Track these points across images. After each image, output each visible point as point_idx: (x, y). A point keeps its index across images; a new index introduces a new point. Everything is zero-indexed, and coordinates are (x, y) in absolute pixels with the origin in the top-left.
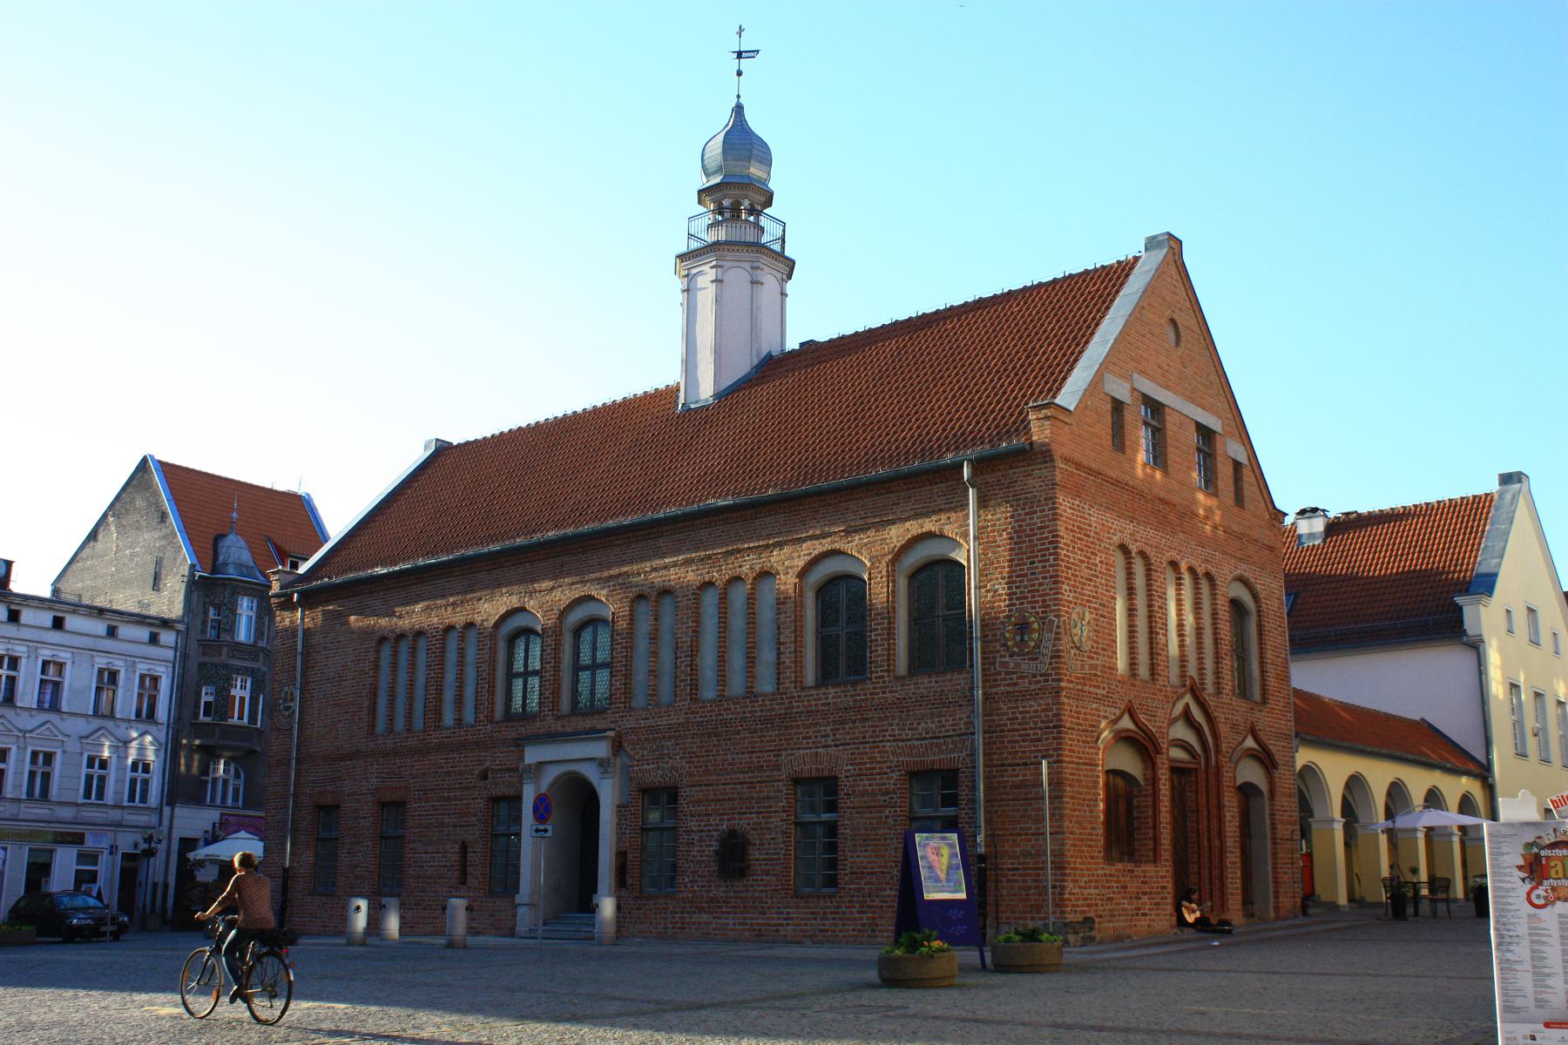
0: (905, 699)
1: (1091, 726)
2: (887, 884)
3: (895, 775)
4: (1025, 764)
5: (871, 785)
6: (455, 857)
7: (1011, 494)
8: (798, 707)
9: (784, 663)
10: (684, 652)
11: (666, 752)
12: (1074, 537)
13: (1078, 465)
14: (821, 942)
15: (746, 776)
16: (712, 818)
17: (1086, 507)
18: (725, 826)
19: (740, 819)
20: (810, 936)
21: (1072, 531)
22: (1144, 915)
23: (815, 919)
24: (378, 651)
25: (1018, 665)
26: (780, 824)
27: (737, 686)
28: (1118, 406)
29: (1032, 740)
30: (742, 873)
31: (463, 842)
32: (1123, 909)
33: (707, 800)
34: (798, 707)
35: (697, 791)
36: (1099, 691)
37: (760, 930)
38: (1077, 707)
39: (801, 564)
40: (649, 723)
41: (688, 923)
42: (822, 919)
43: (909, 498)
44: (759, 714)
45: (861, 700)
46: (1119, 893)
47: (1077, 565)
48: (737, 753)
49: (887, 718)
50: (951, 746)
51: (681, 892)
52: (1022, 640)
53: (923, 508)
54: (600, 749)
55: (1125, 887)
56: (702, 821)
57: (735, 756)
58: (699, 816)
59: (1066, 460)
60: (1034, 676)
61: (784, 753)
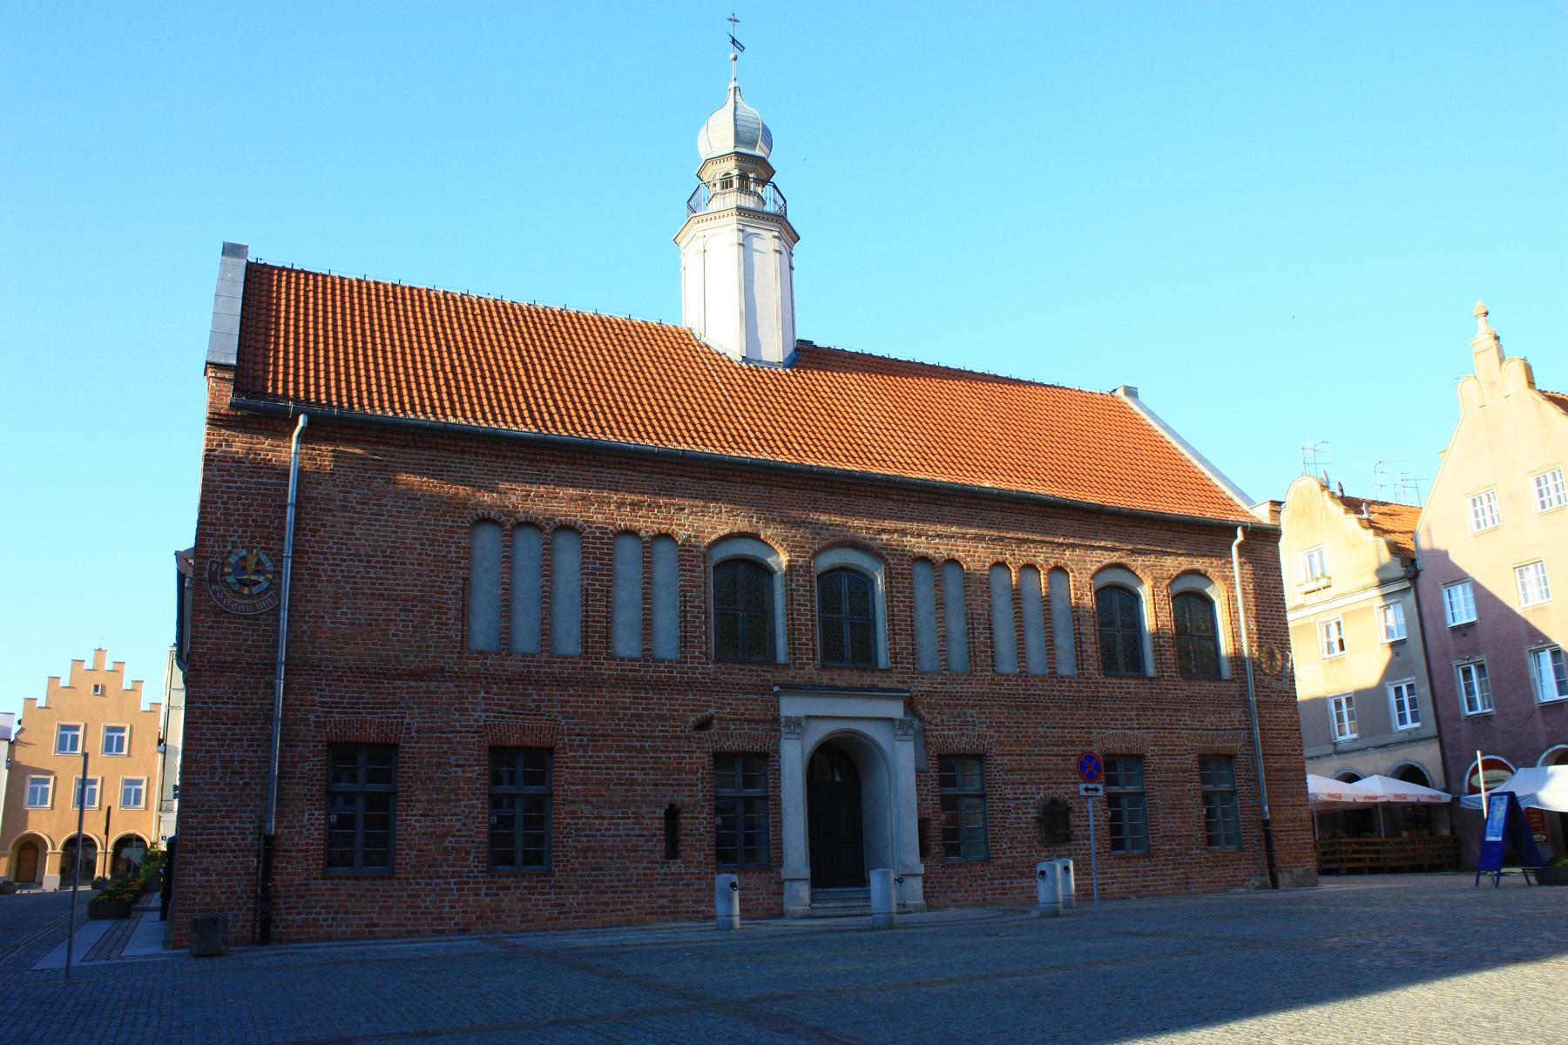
2: (1194, 844)
3: (1192, 757)
6: (659, 824)
9: (1086, 651)
10: (982, 624)
11: (971, 720)
14: (1145, 896)
16: (1028, 786)
18: (1042, 795)
19: (1058, 789)
20: (1135, 892)
23: (1137, 877)
25: (1270, 683)
27: (1036, 663)
29: (1284, 738)
31: (672, 806)
33: (1021, 770)
34: (1104, 692)
35: (1010, 760)
39: (1094, 568)
40: (948, 688)
41: (1010, 889)
42: (1143, 876)
45: (1157, 693)
48: (1048, 728)
49: (1180, 710)
54: (896, 710)
56: (1018, 789)
58: (1013, 784)
60: (1280, 692)
61: (1095, 731)
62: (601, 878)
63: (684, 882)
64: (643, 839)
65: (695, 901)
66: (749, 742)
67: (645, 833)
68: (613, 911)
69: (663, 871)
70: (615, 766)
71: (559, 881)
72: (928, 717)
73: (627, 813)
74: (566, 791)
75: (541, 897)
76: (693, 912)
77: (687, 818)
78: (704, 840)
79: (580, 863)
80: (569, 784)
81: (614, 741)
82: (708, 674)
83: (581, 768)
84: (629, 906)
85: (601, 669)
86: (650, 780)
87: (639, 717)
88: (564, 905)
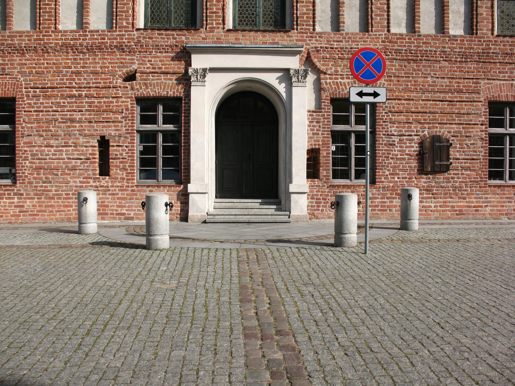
8: (495, 49)
9: (482, 14)
15: (447, 96)
18: (426, 133)
19: (440, 128)
20: (506, 214)
23: (509, 202)
26: (479, 133)
30: (446, 169)
31: (103, 138)
34: (495, 49)
37: (460, 211)
44: (458, 50)
51: (383, 182)
57: (434, 79)
58: (399, 123)
61: (482, 82)
62: (49, 188)
63: (110, 192)
64: (79, 161)
65: (118, 206)
66: (164, 89)
67: (82, 157)
68: (57, 211)
69: (95, 184)
70: (59, 109)
71: (20, 190)
72: (323, 68)
73: (68, 143)
74: (23, 128)
75: (8, 201)
76: (117, 214)
77: (113, 146)
78: (127, 162)
79: (35, 178)
80: (26, 123)
81: (58, 91)
82: (133, 39)
83: (35, 111)
84: (69, 208)
85: (49, 39)
86: (86, 119)
87: (78, 73)
88: (23, 206)
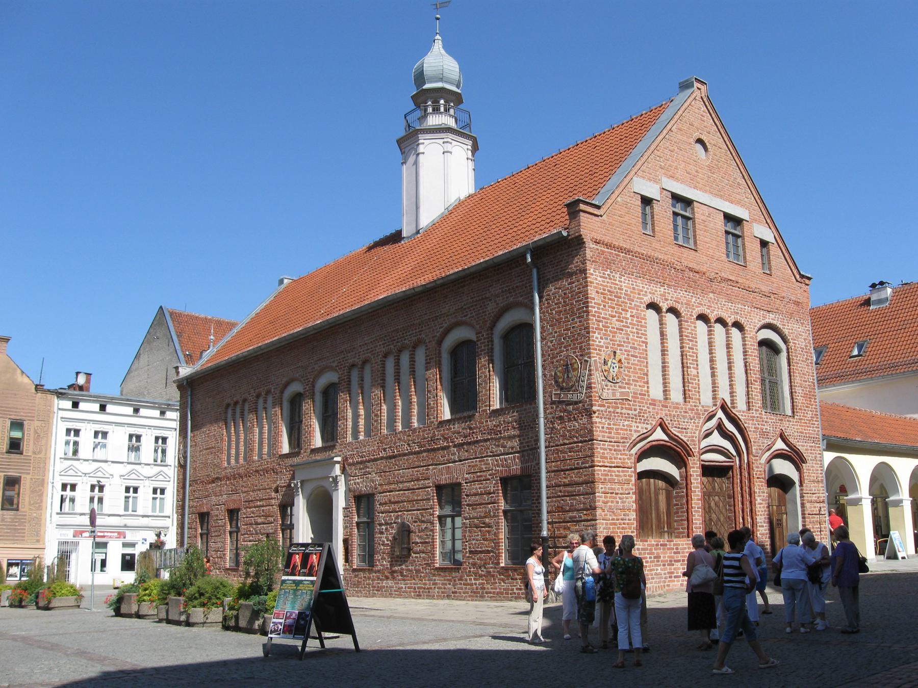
0: (498, 425)
1: (622, 438)
4: (572, 469)
5: (480, 488)
7: (559, 270)
12: (605, 298)
13: (608, 246)
17: (618, 276)
21: (602, 293)
22: (675, 577)
24: (226, 413)
28: (647, 201)
32: (656, 574)
36: (630, 412)
38: (609, 424)
43: (499, 280)
46: (652, 562)
47: (609, 319)
50: (527, 458)
52: (568, 377)
53: (506, 287)
55: (658, 557)
59: (597, 242)
